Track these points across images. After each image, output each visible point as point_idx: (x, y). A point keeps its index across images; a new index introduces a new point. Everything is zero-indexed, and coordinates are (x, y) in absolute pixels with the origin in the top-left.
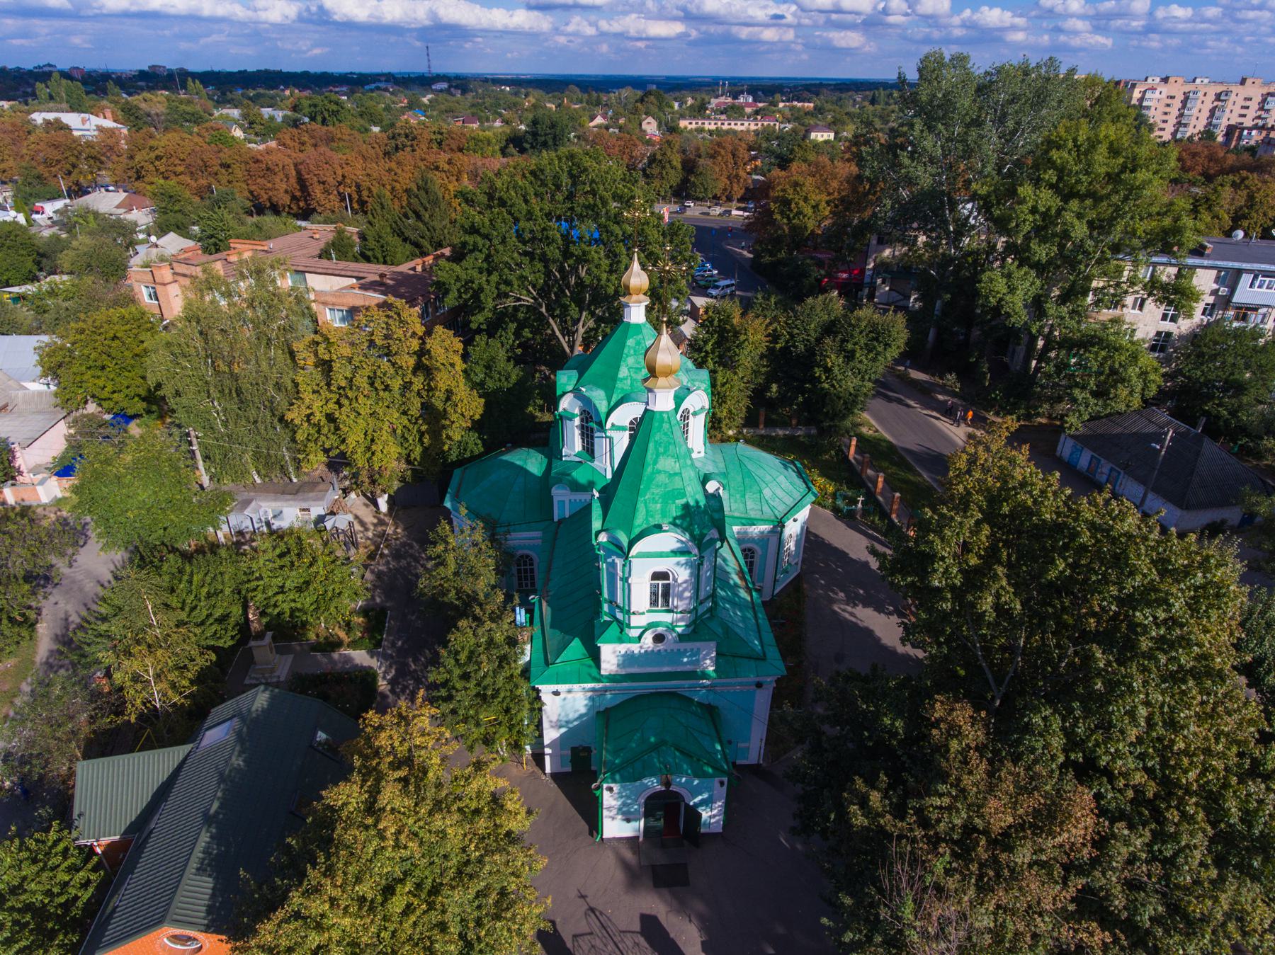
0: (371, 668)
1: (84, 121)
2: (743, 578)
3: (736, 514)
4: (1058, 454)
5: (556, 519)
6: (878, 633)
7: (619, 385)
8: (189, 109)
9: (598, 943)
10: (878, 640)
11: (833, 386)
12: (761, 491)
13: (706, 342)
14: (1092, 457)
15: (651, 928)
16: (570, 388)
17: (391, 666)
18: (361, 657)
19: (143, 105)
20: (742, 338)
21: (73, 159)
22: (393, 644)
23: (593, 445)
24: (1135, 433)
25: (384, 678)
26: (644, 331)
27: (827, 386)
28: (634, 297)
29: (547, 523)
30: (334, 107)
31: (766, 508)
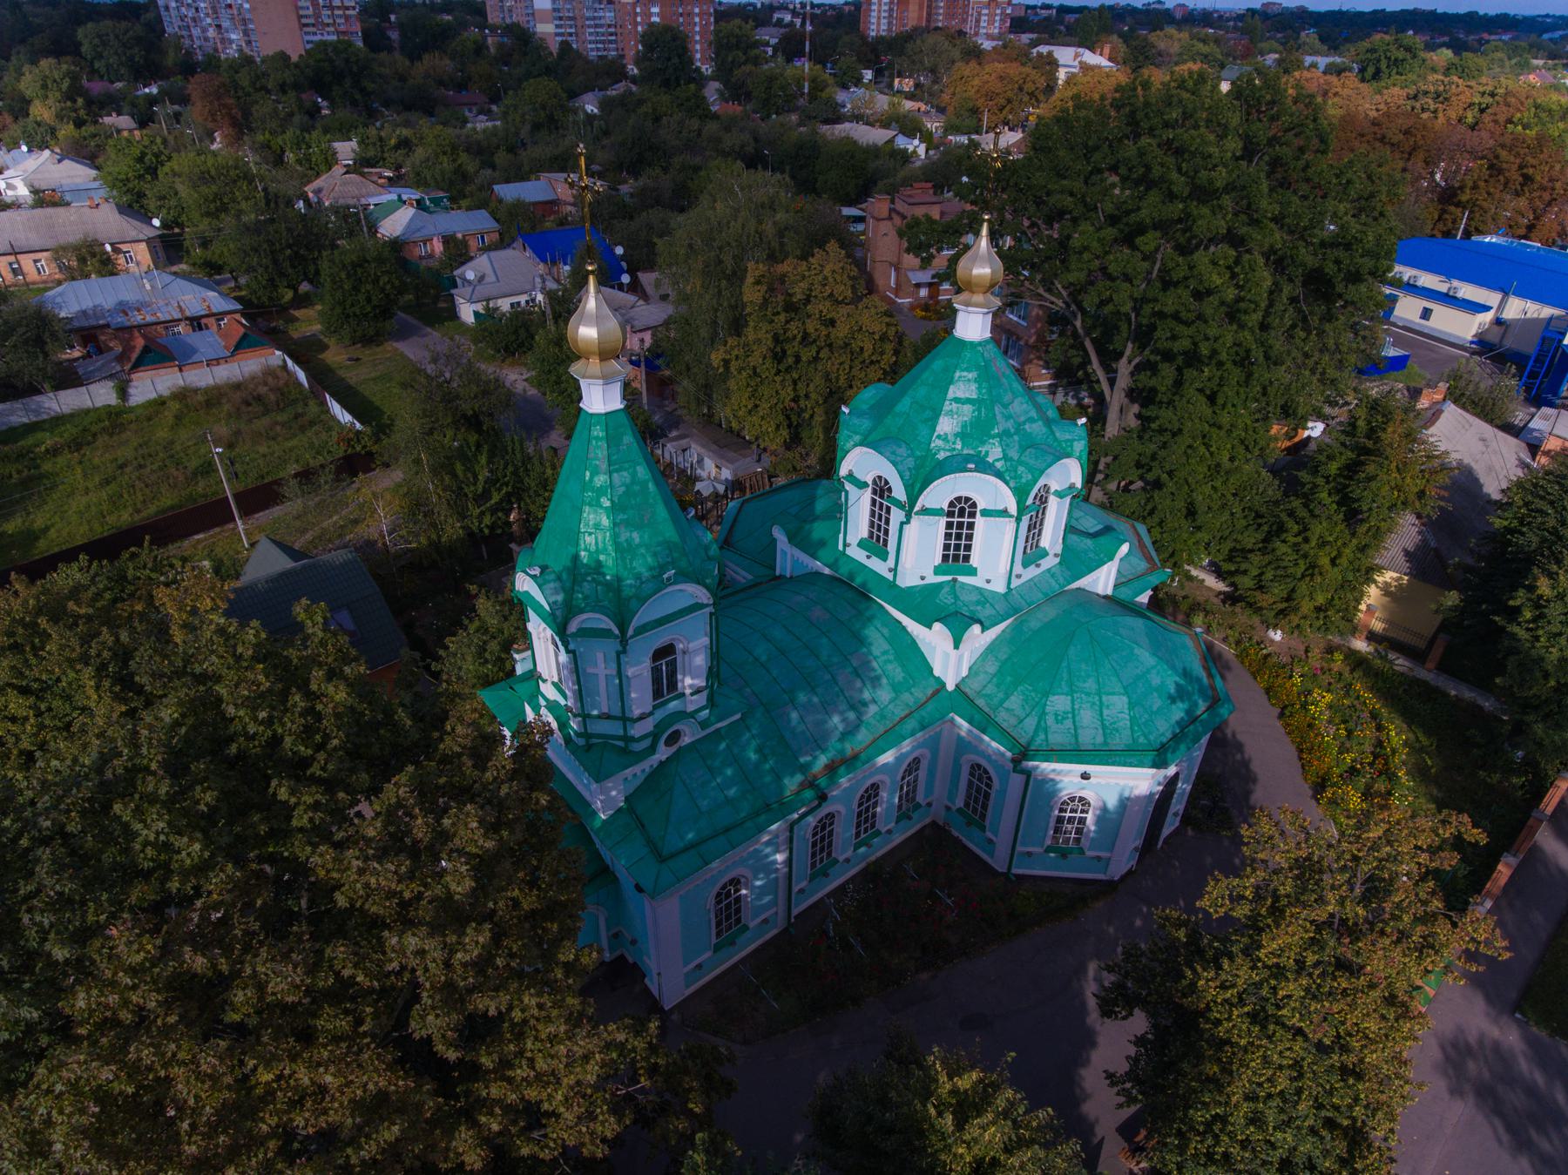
1: (1077, 55)
2: (831, 769)
3: (980, 702)
7: (889, 420)
8: (1204, 49)
11: (1537, 638)
12: (1046, 694)
13: (1331, 458)
19: (1162, 45)
20: (1371, 469)
21: (1009, 94)
26: (967, 354)
27: (1521, 633)
28: (964, 296)
30: (1401, 54)
31: (1030, 724)
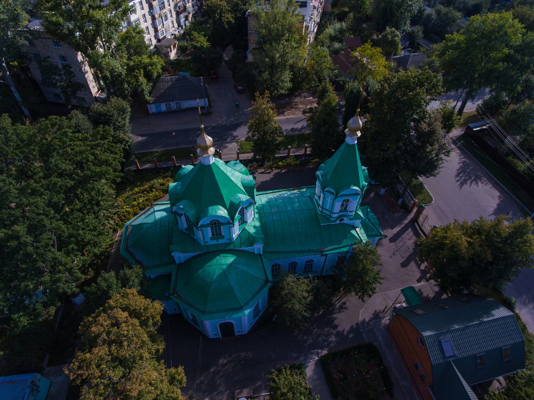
0: (316, 363)
4: (151, 112)
5: (262, 253)
6: (264, 180)
9: (402, 252)
10: (267, 181)
11: (129, 145)
14: (166, 104)
15: (393, 239)
16: (226, 211)
17: (312, 353)
18: (310, 370)
22: (297, 358)
23: (244, 219)
24: (168, 88)
25: (321, 352)
29: (263, 257)
